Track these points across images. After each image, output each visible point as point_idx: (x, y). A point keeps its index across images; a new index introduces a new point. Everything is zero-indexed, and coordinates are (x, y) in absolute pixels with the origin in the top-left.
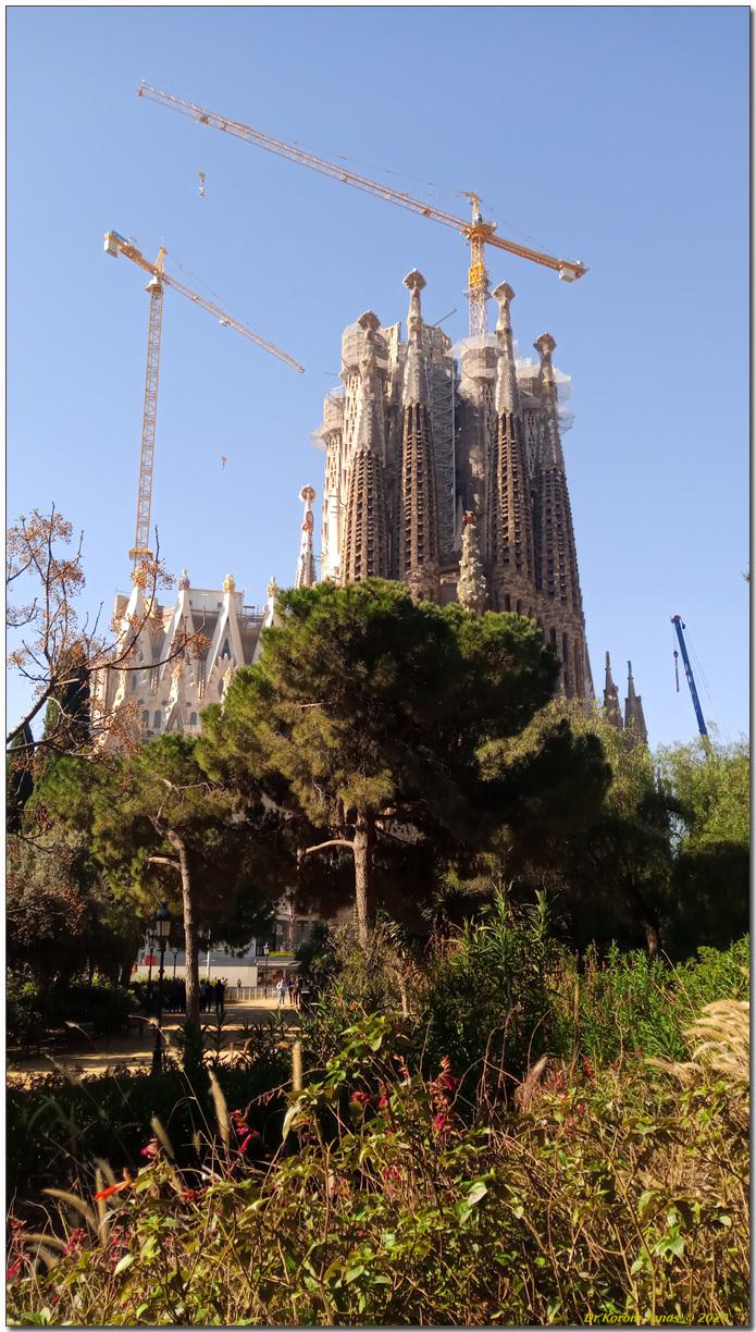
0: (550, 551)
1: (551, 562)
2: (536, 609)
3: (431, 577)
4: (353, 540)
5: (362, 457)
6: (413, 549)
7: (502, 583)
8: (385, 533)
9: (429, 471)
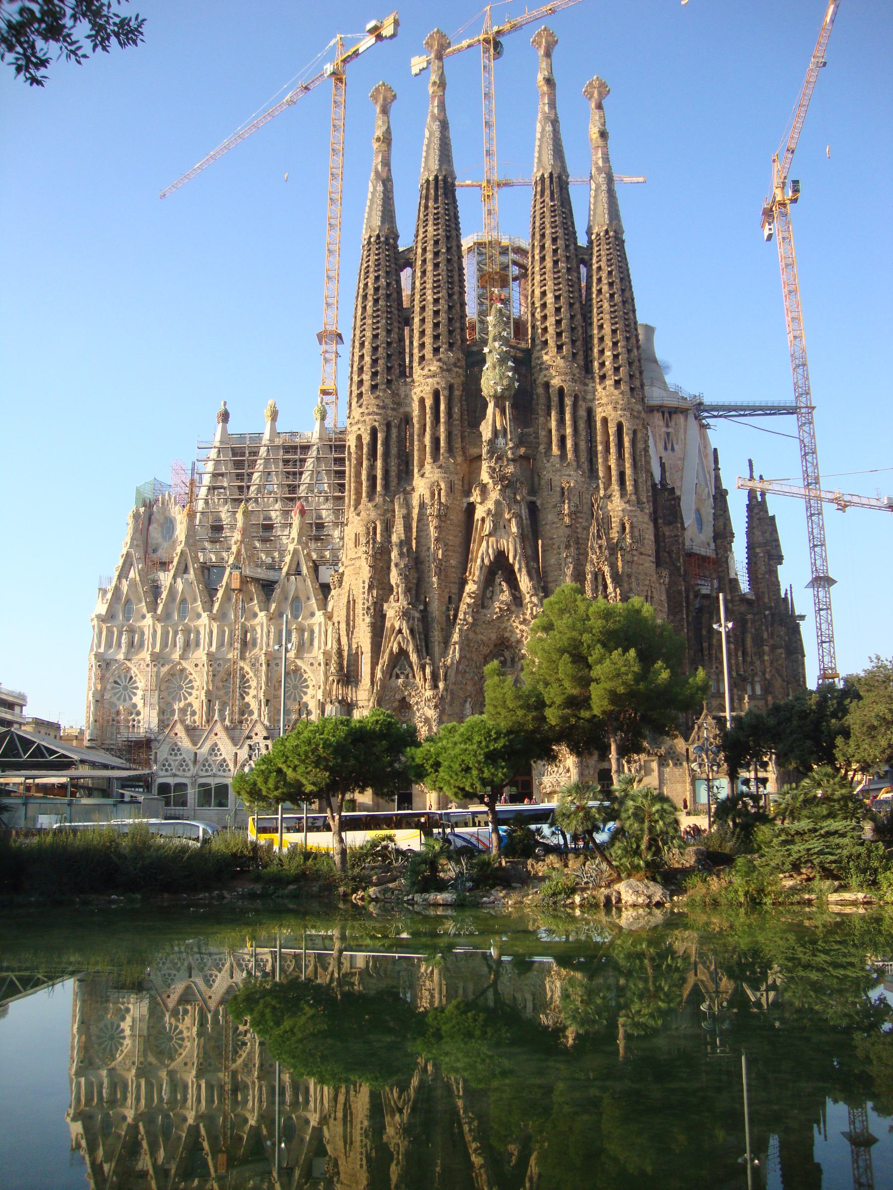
0: (601, 327)
1: (601, 339)
2: (584, 399)
3: (448, 370)
4: (357, 337)
5: (369, 243)
6: (428, 340)
7: (541, 370)
8: (396, 324)
9: (449, 249)
